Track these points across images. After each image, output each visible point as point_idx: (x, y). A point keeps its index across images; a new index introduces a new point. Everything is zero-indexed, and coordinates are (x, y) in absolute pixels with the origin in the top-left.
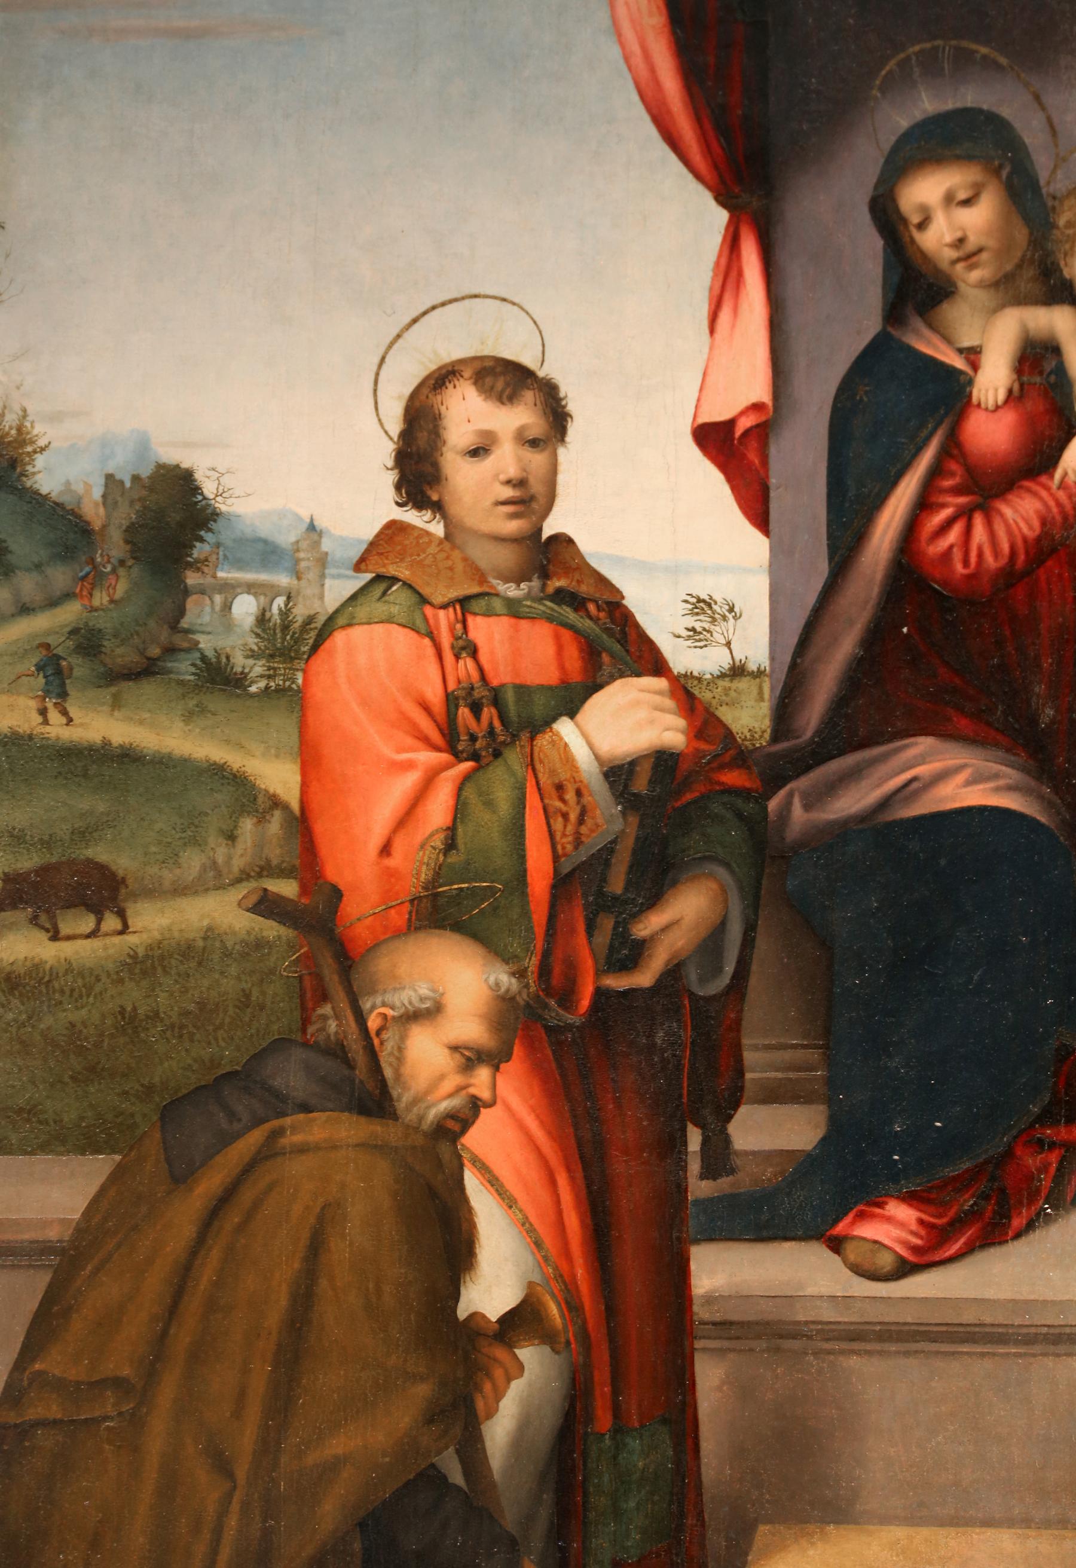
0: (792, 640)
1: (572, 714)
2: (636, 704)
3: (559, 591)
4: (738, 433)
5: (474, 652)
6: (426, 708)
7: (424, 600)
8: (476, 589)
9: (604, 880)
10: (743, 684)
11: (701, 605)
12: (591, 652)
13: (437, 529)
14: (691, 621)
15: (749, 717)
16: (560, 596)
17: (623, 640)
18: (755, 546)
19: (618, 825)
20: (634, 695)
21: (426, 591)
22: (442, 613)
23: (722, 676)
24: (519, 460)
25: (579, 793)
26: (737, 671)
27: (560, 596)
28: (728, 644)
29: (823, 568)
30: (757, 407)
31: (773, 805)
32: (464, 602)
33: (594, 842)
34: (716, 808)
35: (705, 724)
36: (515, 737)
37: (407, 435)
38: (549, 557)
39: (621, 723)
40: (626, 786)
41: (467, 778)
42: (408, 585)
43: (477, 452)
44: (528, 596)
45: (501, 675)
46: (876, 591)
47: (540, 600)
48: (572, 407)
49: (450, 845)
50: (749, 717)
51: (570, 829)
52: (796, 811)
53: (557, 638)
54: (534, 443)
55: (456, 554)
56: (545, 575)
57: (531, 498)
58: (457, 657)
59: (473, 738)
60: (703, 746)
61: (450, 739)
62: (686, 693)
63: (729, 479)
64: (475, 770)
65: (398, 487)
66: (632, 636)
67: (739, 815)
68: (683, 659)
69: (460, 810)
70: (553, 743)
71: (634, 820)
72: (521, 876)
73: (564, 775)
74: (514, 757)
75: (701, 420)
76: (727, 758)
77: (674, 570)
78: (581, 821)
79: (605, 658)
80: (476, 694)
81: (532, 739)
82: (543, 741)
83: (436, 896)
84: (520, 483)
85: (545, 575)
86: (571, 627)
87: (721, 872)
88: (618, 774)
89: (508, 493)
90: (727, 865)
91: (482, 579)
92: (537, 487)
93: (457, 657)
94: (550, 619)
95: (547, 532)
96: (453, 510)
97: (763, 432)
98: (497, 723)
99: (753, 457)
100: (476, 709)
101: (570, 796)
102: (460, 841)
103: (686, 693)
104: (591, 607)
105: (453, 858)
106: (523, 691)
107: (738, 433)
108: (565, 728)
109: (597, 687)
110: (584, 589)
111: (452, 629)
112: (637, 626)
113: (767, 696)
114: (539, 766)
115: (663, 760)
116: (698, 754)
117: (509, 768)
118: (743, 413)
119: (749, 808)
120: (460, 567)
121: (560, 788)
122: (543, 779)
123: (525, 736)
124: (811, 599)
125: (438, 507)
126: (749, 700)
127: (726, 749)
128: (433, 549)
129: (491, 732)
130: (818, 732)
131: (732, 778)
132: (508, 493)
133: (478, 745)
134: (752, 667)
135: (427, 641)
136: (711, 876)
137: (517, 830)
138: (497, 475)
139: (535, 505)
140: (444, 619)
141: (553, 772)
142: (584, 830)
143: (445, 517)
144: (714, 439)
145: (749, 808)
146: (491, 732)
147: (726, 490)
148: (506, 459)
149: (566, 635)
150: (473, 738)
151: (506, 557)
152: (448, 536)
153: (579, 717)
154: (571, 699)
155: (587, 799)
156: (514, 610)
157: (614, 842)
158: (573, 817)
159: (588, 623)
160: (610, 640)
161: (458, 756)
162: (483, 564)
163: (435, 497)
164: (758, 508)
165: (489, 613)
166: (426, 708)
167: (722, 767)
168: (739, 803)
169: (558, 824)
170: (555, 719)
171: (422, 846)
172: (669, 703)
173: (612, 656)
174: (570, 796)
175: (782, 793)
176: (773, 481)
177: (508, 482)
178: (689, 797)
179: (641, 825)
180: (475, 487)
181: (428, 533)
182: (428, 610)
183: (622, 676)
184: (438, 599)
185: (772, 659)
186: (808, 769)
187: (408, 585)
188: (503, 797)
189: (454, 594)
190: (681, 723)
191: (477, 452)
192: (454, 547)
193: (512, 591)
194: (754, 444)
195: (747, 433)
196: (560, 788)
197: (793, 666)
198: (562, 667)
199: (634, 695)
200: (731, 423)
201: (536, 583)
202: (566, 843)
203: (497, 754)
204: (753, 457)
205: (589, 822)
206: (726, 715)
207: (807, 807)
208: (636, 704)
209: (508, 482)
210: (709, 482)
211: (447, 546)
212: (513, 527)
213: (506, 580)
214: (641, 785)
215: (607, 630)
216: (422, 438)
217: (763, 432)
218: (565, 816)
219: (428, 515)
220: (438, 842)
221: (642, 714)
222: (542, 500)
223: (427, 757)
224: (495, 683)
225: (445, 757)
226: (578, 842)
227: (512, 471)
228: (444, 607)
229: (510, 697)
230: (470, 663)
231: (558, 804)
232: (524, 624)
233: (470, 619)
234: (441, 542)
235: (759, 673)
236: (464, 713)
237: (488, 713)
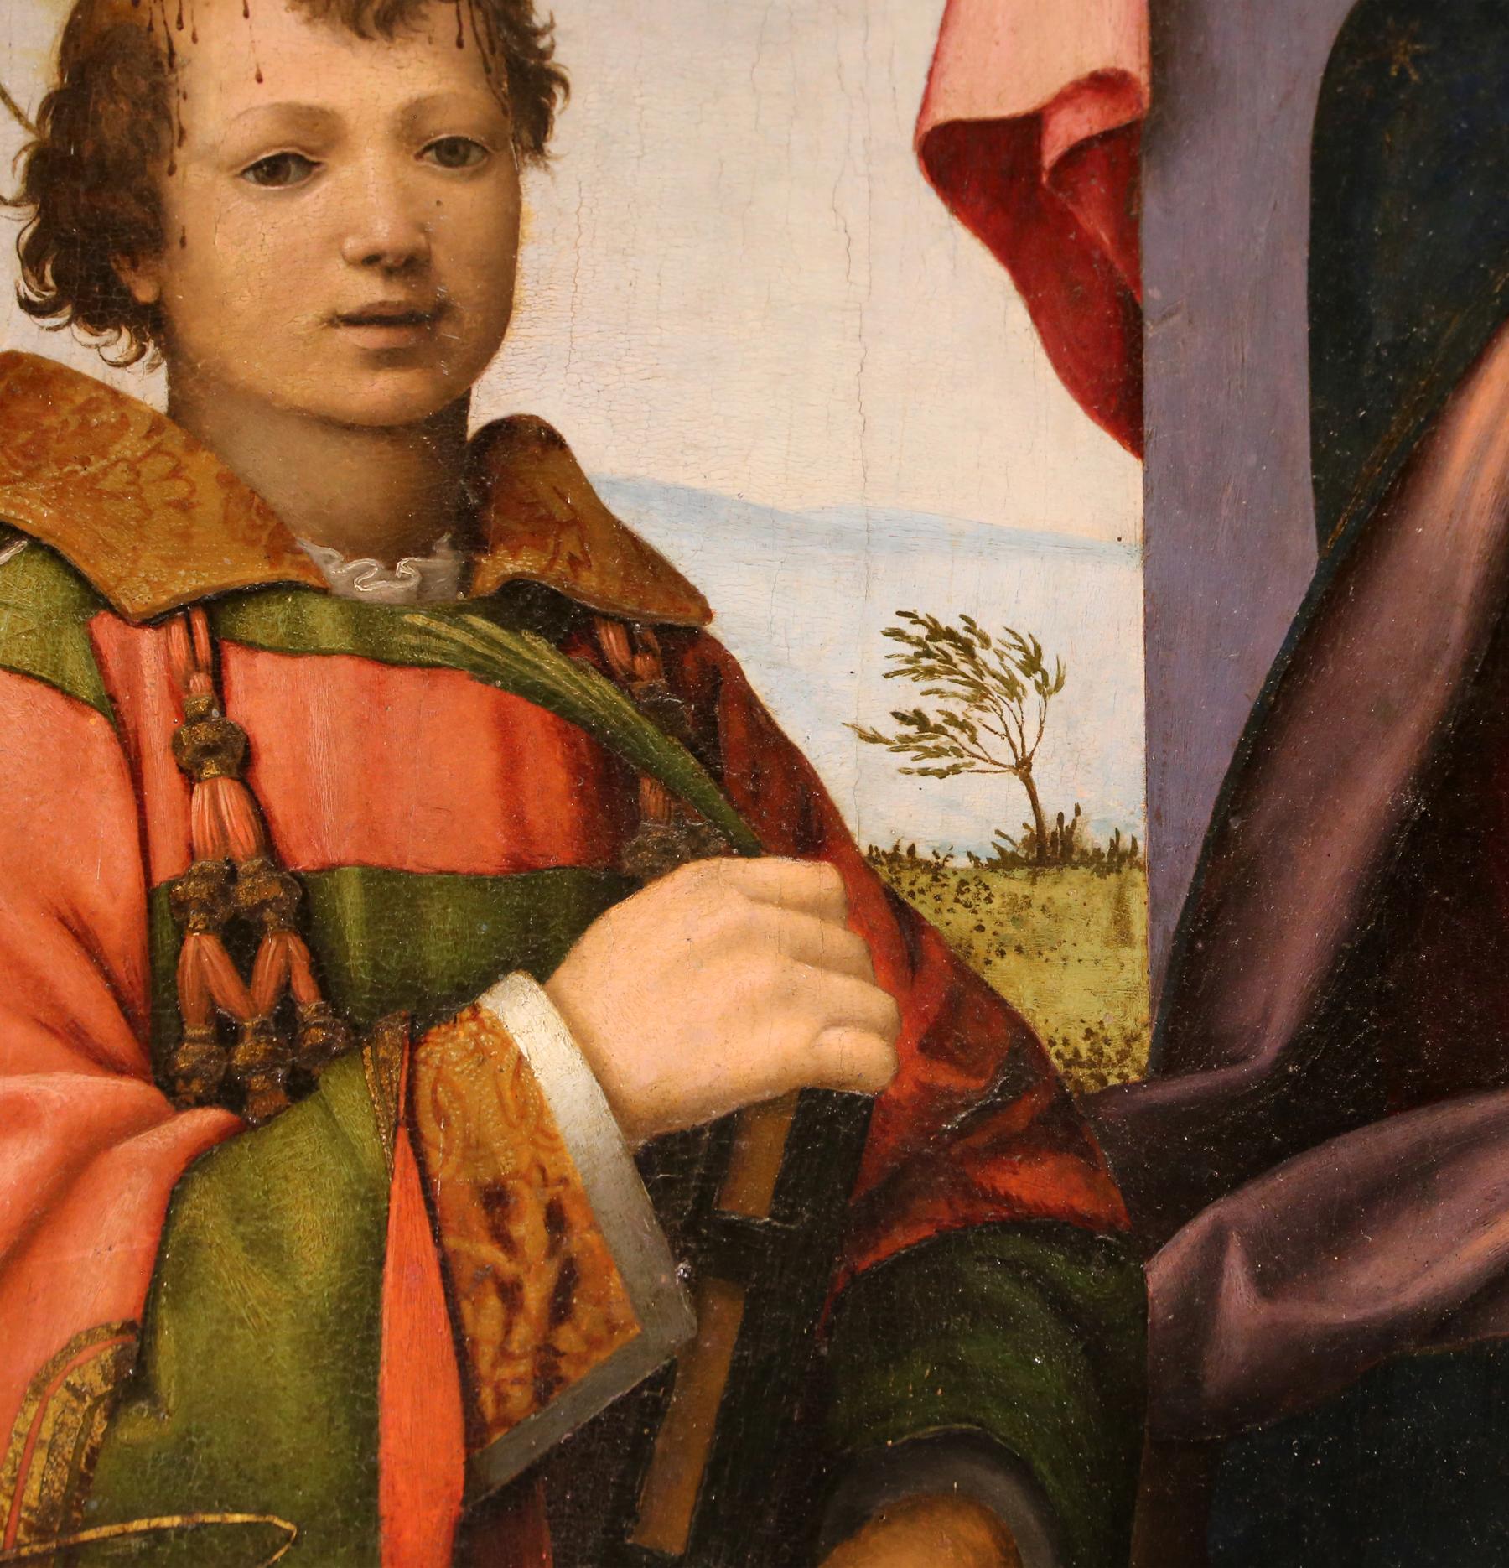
0: (1215, 761)
1: (542, 968)
2: (742, 939)
3: (513, 587)
4: (1051, 155)
5: (242, 761)
6: (80, 933)
7: (93, 598)
8: (258, 572)
9: (626, 1507)
10: (1067, 889)
11: (941, 647)
12: (607, 773)
13: (148, 386)
14: (910, 695)
15: (1087, 990)
16: (518, 604)
17: (705, 743)
18: (1096, 482)
19: (678, 1326)
20: (734, 911)
21: (102, 571)
22: (148, 639)
23: (1006, 862)
24: (406, 197)
25: (555, 1218)
26: (1051, 848)
27: (518, 604)
28: (1023, 767)
29: (1302, 552)
30: (1106, 84)
31: (1162, 1271)
32: (218, 607)
33: (598, 1375)
34: (987, 1279)
35: (953, 1007)
36: (359, 1034)
37: (68, 107)
38: (486, 487)
39: (695, 998)
40: (704, 1200)
41: (199, 1159)
42: (45, 550)
43: (281, 167)
44: (420, 598)
45: (322, 836)
46: (1458, 623)
47: (454, 613)
48: (565, 57)
49: (133, 1382)
50: (1087, 990)
51: (523, 1332)
52: (1228, 1288)
53: (504, 729)
54: (452, 152)
55: (202, 465)
56: (474, 540)
57: (439, 310)
58: (190, 777)
59: (226, 1033)
60: (946, 1078)
61: (153, 1035)
62: (891, 910)
63: (1024, 285)
64: (228, 1136)
65: (31, 257)
66: (734, 730)
67: (1060, 1303)
68: (883, 803)
69: (168, 1267)
70: (480, 1054)
71: (727, 1312)
72: (361, 1492)
73: (510, 1159)
74: (352, 1097)
75: (942, 114)
76: (1019, 1119)
77: (864, 541)
78: (559, 1310)
79: (650, 795)
80: (244, 894)
81: (414, 1043)
82: (447, 1049)
83: (71, 1554)
84: (407, 265)
85: (474, 540)
86: (546, 697)
87: (1001, 1487)
88: (681, 1159)
89: (369, 290)
90: (1021, 1469)
91: (280, 543)
92: (456, 279)
93: (190, 777)
94: (483, 671)
95: (482, 413)
96: (201, 332)
97: (1121, 156)
98: (304, 988)
99: (1095, 223)
100: (240, 940)
101: (528, 1228)
102: (166, 1368)
103: (891, 910)
104: (612, 640)
105: (138, 1428)
106: (391, 887)
107: (1051, 155)
108: (520, 1011)
109: (624, 885)
110: (589, 584)
111: (177, 691)
112: (748, 701)
113: (1139, 928)
114: (431, 1129)
115: (820, 1116)
116: (929, 1099)
117: (335, 1131)
118: (1064, 98)
119: (1086, 1280)
120: (211, 500)
121: (496, 1199)
122: (444, 1168)
123: (392, 1032)
124: (1269, 642)
125: (153, 324)
126: (1086, 940)
127: (1015, 1090)
128: (130, 445)
129: (286, 1015)
130: (1296, 1047)
131: (1036, 1182)
132: (369, 290)
133: (241, 1055)
134: (1094, 837)
135: (96, 724)
136: (971, 1500)
137: (350, 1337)
138: (336, 239)
139: (448, 332)
140: (153, 658)
141: (475, 1149)
142: (568, 1338)
143: (172, 352)
144: (978, 166)
145: (1086, 1280)
146: (286, 1015)
147: (1012, 315)
148: (366, 193)
149: (532, 719)
150: (226, 1033)
151: (352, 479)
152: (179, 409)
153: (564, 976)
154: (540, 922)
155: (580, 1239)
156: (374, 641)
157: (663, 1380)
158: (535, 1295)
159: (600, 688)
160: (668, 748)
161: (176, 1092)
162: (283, 498)
163: (145, 293)
164: (1111, 380)
165: (293, 648)
166: (80, 933)
167: (1003, 1148)
168: (1057, 1261)
169: (486, 1319)
170: (487, 980)
171: (38, 1388)
172: (843, 940)
173: (672, 789)
174: (528, 1228)
175: (1191, 1234)
176: (1152, 295)
177: (371, 261)
178: (901, 1239)
179: (751, 1330)
180: (268, 271)
181: (118, 397)
182: (107, 630)
183: (699, 851)
184: (139, 598)
185: (1155, 814)
186: (1268, 1160)
187: (45, 550)
188: (313, 1223)
189: (187, 583)
190: (879, 1003)
191: (281, 167)
192: (196, 442)
193: (369, 581)
194: (1096, 187)
195: (1076, 154)
196: (496, 1199)
197: (1218, 840)
198: (515, 820)
199: (734, 911)
200: (1031, 125)
201: (444, 561)
202: (508, 1380)
203: (301, 1087)
204: (1095, 223)
205: (585, 1312)
206: (1016, 982)
207: (1267, 1284)
208: (742, 939)
209: (371, 261)
210: (967, 290)
211: (174, 438)
212: (381, 391)
213: (354, 548)
214: (751, 1196)
215: (656, 712)
216: (114, 120)
217: (1121, 156)
218: (510, 1293)
219: (120, 343)
220: (92, 1375)
221: (761, 971)
222: (470, 317)
223: (73, 1091)
224: (305, 860)
225: (132, 1091)
226: (547, 1378)
227: (384, 230)
228: (157, 620)
229: (350, 903)
230: (229, 795)
231: (489, 1252)
232: (403, 683)
233: (236, 662)
234: (156, 425)
235: (1116, 859)
236: (202, 952)
237: (278, 953)
